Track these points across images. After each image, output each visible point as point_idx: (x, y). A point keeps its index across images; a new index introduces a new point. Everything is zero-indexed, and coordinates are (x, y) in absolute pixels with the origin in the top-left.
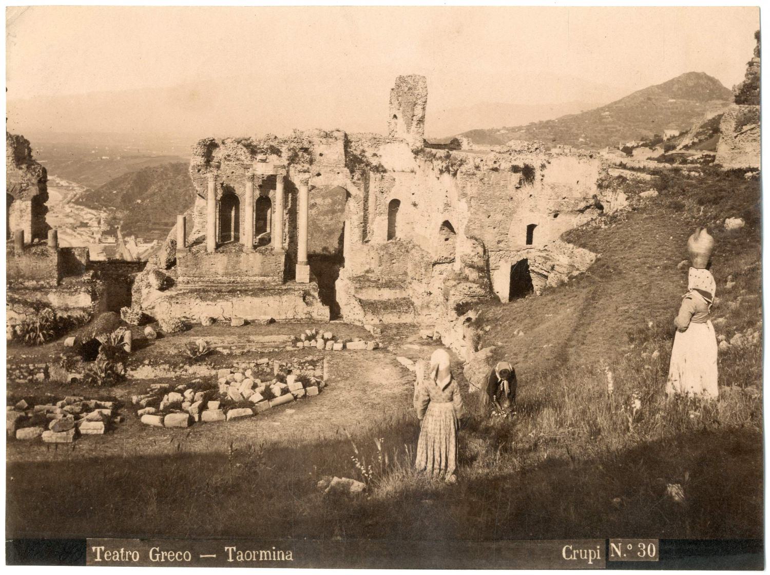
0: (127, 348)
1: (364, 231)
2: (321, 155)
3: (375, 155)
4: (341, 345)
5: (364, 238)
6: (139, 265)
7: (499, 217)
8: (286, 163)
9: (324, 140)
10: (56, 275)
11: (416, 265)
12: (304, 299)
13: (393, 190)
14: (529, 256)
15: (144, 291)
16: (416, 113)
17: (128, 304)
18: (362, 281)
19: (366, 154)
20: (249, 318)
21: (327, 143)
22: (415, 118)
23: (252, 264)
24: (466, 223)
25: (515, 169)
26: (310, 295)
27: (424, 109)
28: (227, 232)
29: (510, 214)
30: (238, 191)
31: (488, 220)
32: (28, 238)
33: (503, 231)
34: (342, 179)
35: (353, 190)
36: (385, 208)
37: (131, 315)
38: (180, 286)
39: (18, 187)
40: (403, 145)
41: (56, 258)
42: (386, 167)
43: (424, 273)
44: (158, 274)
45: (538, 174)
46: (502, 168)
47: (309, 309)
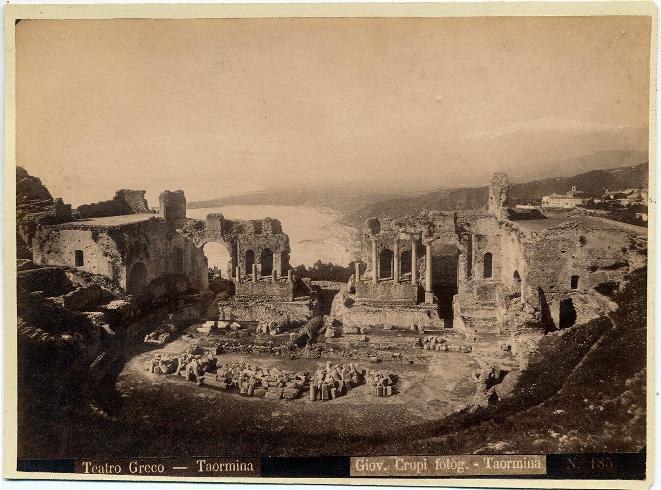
1: (468, 272)
2: (440, 226)
6: (337, 292)
7: (550, 271)
9: (442, 217)
10: (292, 295)
11: (500, 296)
16: (502, 198)
17: (329, 314)
20: (395, 324)
21: (444, 220)
22: (501, 201)
23: (398, 292)
24: (527, 274)
28: (385, 270)
30: (391, 249)
31: (542, 273)
32: (279, 272)
33: (554, 280)
34: (454, 241)
35: (461, 247)
36: (480, 258)
37: (329, 320)
39: (275, 247)
40: (493, 219)
41: (292, 285)
43: (504, 302)
44: (344, 296)
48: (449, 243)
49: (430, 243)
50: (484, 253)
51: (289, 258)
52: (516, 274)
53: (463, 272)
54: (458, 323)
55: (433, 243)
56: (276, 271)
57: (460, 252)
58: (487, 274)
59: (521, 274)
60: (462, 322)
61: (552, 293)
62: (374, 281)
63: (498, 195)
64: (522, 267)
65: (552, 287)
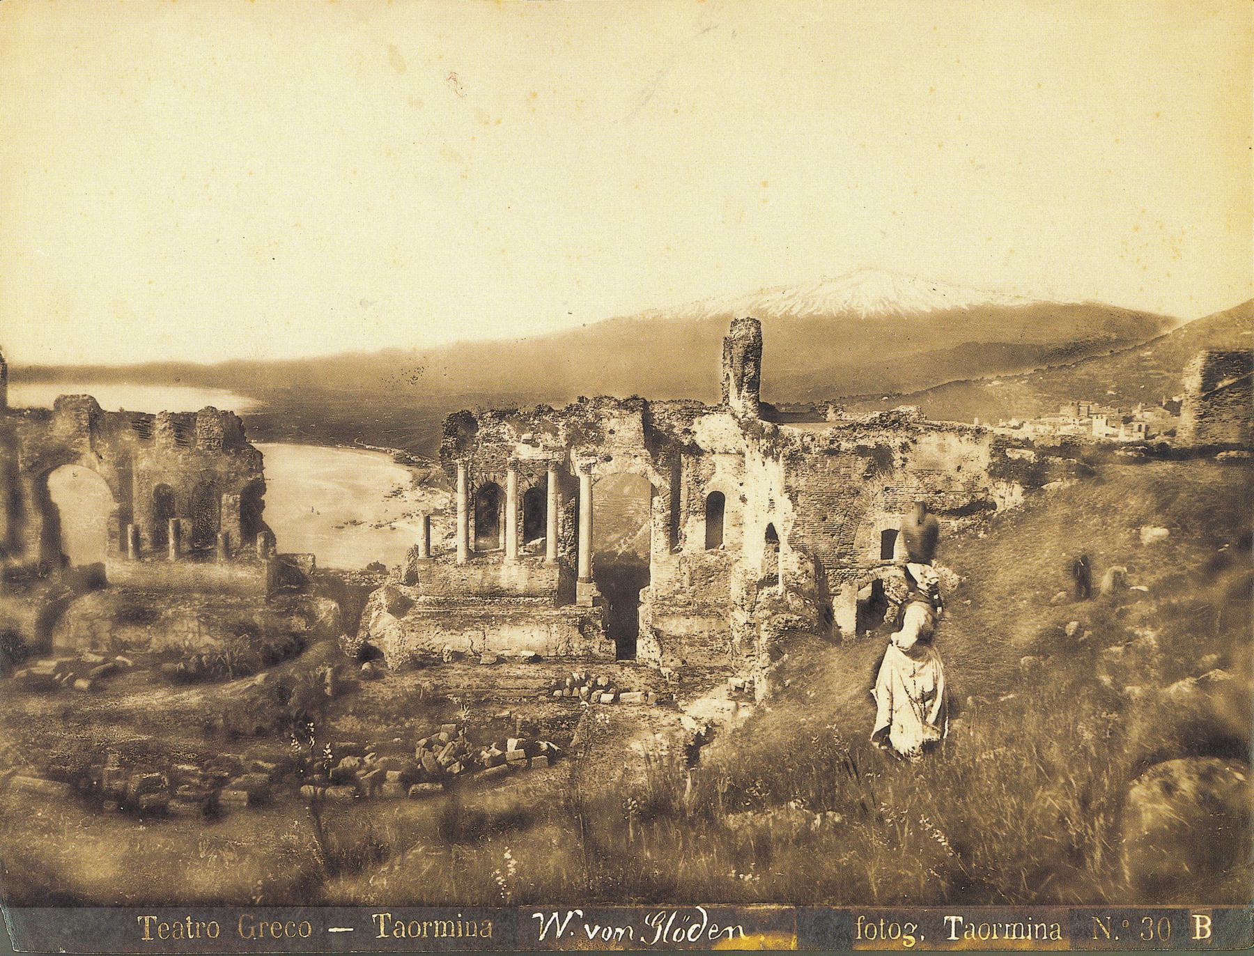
0: (328, 691)
2: (612, 432)
3: (687, 431)
4: (611, 697)
5: (671, 548)
7: (839, 519)
8: (564, 444)
9: (616, 413)
12: (581, 630)
13: (714, 480)
14: (884, 576)
15: (374, 614)
18: (665, 606)
19: (675, 431)
25: (862, 451)
26: (590, 623)
27: (757, 366)
29: (856, 516)
35: (657, 480)
36: (698, 505)
38: (420, 609)
42: (702, 446)
45: (897, 456)
46: (842, 449)
47: (587, 643)
48: (633, 470)
49: (587, 469)
50: (707, 492)
51: (262, 505)
52: (771, 534)
53: (662, 535)
54: (645, 648)
55: (594, 470)
56: (227, 537)
57: (654, 491)
58: (713, 540)
59: (779, 530)
60: (654, 646)
61: (842, 568)
62: (461, 556)
63: (737, 365)
64: (783, 517)
65: (841, 555)
